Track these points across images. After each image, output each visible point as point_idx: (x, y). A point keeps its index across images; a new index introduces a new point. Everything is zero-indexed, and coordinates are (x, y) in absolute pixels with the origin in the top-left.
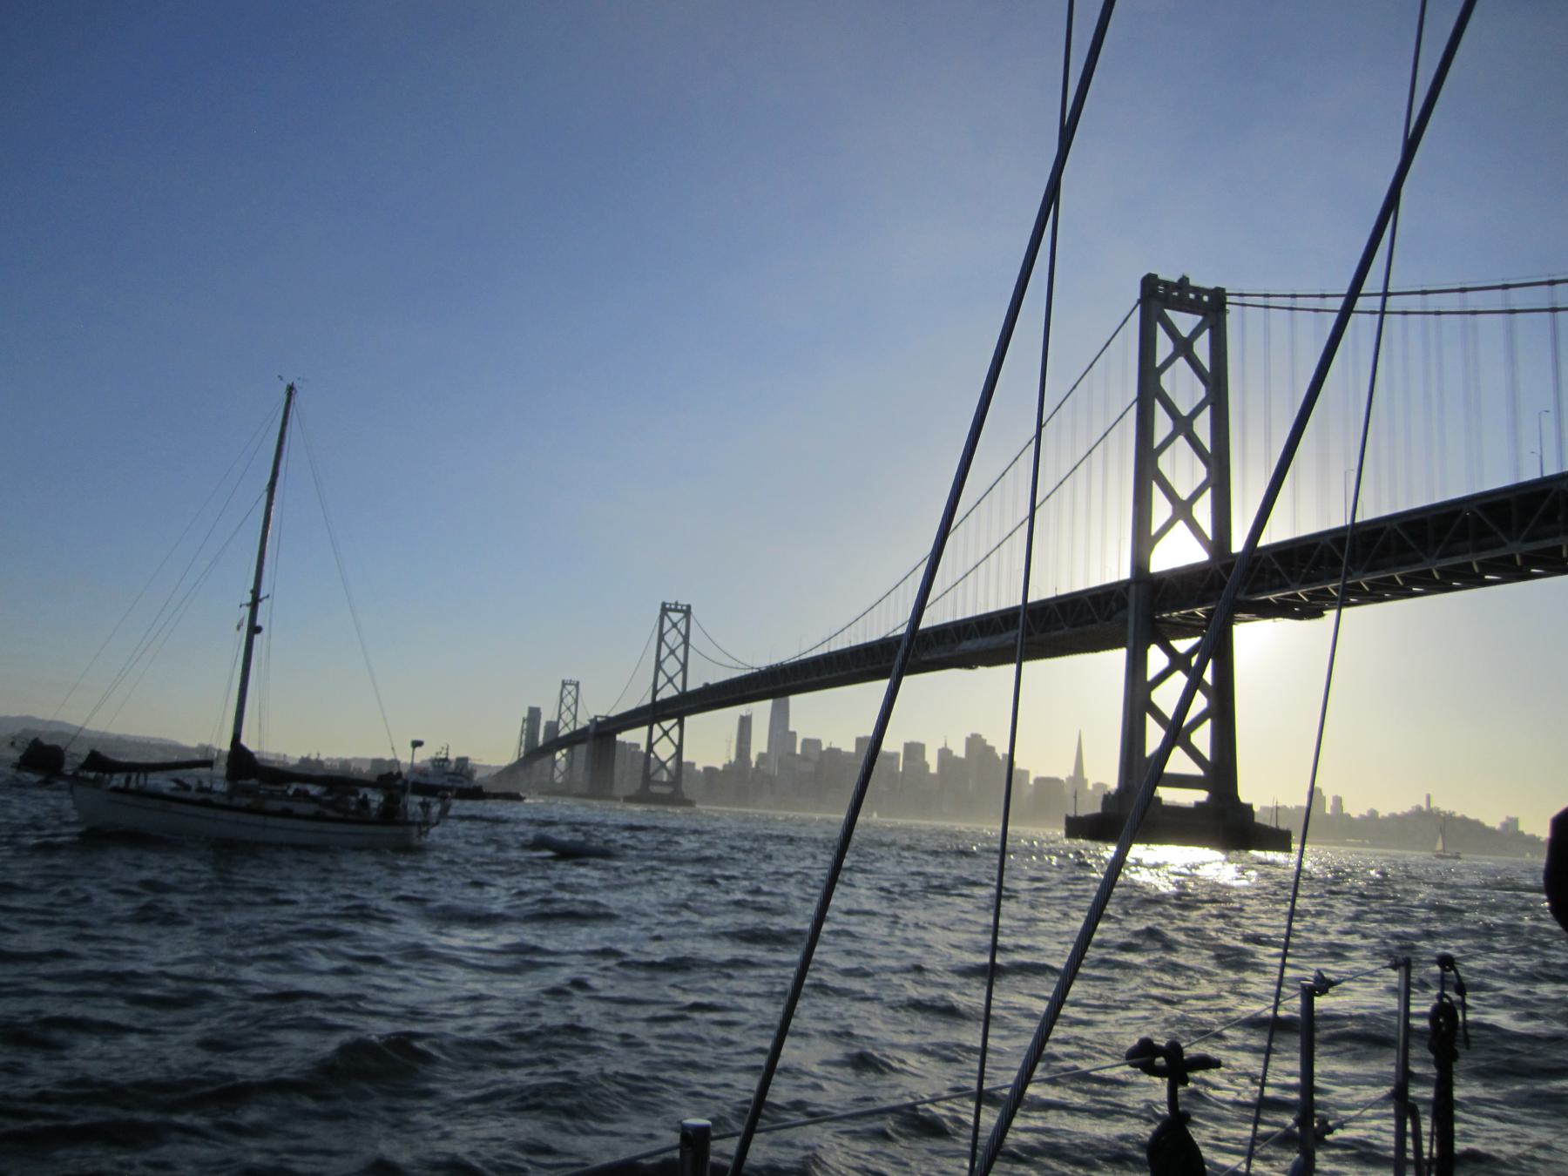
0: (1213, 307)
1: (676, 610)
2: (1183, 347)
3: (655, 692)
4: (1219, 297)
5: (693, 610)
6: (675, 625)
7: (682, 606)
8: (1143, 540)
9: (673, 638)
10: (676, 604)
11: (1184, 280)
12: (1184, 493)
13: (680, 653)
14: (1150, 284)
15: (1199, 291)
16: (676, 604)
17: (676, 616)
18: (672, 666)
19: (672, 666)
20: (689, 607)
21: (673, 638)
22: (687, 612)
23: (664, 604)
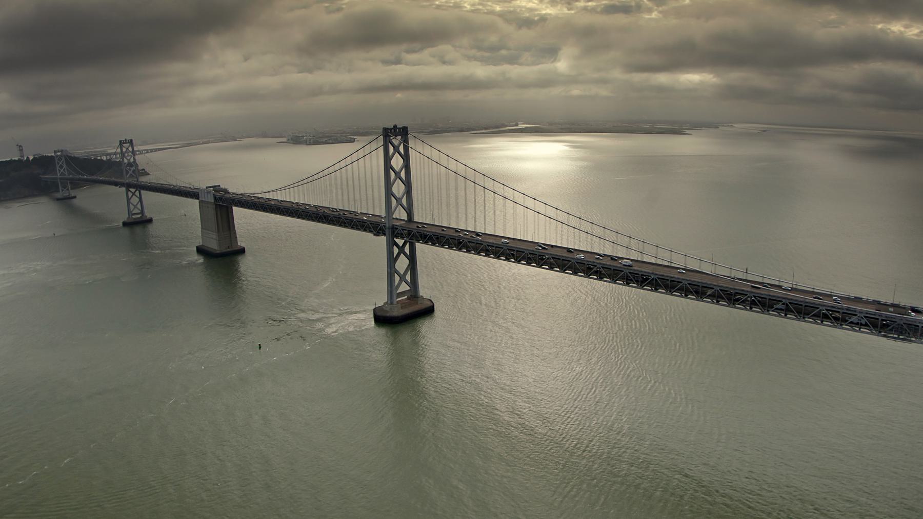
10: (126, 140)
11: (395, 126)
15: (399, 129)
16: (126, 140)
17: (126, 145)
20: (131, 140)
22: (131, 142)
23: (120, 141)
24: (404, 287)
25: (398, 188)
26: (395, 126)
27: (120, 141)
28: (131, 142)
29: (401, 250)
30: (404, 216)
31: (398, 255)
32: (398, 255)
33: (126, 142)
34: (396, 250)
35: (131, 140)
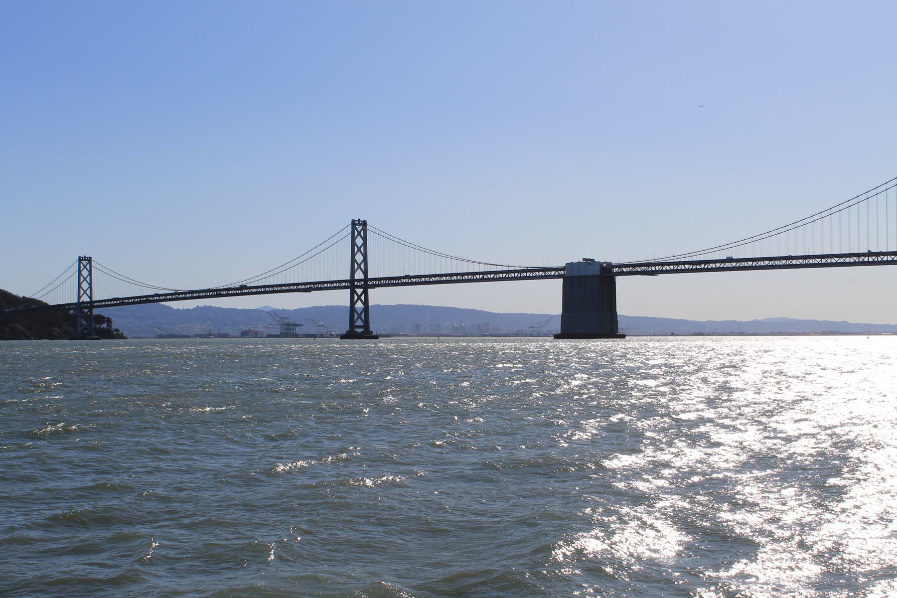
0: (364, 224)
1: (85, 260)
2: (359, 233)
3: (79, 297)
4: (365, 222)
5: (92, 259)
6: (85, 267)
7: (87, 258)
8: (353, 272)
9: (85, 273)
10: (85, 257)
11: (359, 220)
12: (359, 262)
13: (88, 279)
14: (353, 221)
15: (361, 221)
16: (85, 257)
18: (85, 286)
19: (85, 286)
20: (90, 258)
21: (85, 273)
22: (89, 260)
23: (80, 257)
24: (359, 323)
25: (359, 258)
26: (359, 220)
27: (80, 257)
28: (89, 260)
29: (359, 297)
30: (362, 277)
31: (357, 301)
32: (357, 301)
33: (85, 259)
34: (356, 297)
35: (90, 258)
